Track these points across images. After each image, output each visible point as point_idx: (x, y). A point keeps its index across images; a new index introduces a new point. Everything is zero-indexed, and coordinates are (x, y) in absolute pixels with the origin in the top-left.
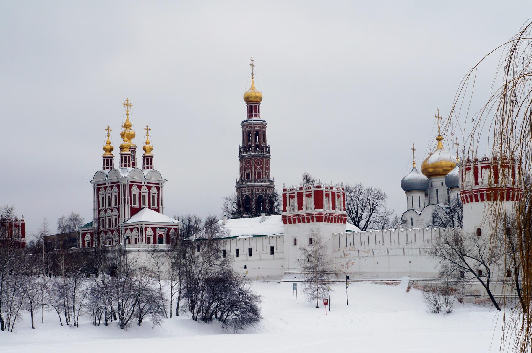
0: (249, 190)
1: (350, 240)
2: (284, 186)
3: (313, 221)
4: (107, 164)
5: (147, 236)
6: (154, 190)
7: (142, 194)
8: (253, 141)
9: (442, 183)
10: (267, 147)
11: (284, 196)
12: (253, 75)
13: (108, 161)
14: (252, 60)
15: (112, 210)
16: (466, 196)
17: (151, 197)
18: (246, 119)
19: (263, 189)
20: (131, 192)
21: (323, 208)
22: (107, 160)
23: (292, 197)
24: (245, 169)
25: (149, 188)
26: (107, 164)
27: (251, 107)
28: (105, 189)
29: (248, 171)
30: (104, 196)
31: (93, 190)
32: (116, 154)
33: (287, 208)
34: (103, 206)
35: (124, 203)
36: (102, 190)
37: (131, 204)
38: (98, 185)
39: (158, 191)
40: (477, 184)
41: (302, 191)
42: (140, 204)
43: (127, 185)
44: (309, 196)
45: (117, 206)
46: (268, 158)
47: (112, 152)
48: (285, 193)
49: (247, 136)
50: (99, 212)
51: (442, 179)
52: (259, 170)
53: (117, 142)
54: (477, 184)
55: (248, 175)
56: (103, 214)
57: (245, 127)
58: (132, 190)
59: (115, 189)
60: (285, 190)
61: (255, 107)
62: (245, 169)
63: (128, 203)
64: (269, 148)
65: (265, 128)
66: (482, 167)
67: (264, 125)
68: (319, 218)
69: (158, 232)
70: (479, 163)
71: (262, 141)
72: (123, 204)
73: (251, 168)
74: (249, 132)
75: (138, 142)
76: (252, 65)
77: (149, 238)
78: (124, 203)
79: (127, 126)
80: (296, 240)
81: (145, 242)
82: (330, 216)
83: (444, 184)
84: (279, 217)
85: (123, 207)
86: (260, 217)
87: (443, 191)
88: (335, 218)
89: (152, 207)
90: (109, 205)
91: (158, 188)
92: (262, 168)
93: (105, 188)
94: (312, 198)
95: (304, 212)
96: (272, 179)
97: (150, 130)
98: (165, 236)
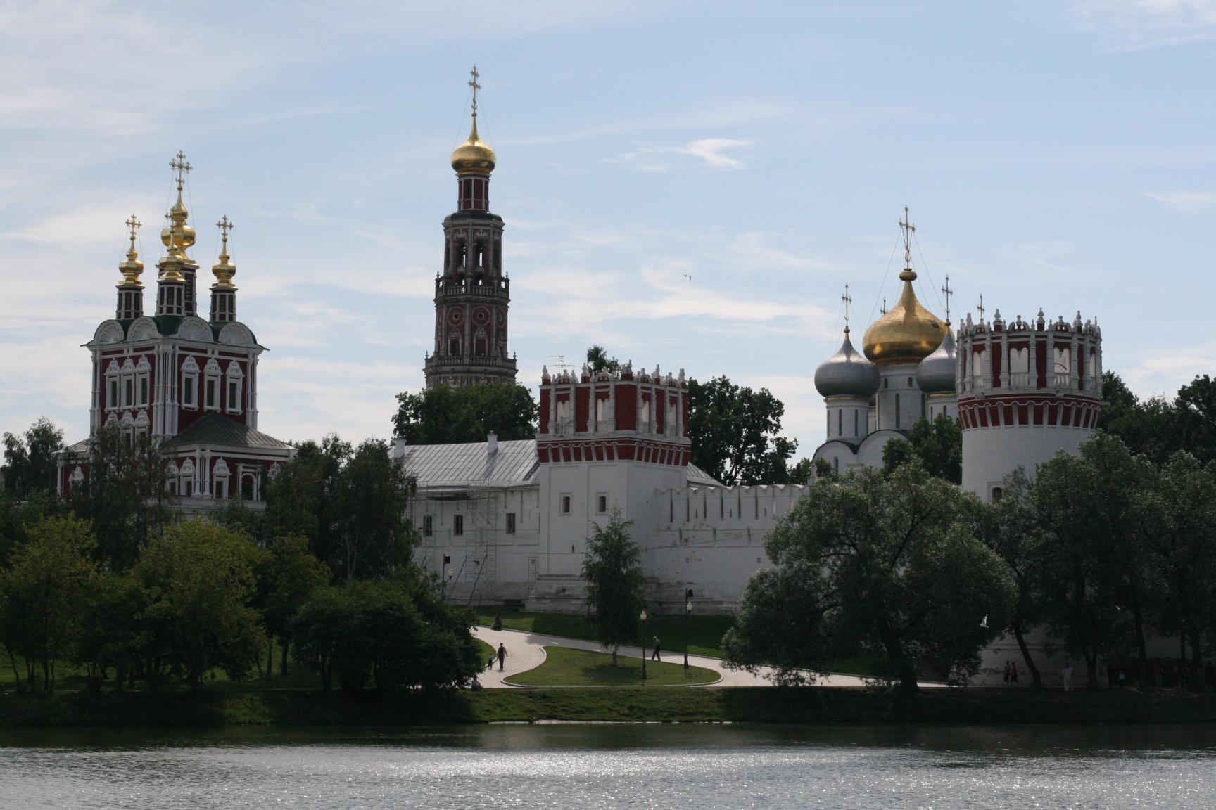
0: (456, 379)
1: (696, 505)
2: (545, 371)
3: (611, 457)
4: (128, 306)
5: (215, 479)
6: (234, 369)
7: (206, 379)
8: (470, 264)
9: (910, 379)
10: (503, 279)
11: (545, 394)
12: (474, 108)
13: (130, 296)
14: (475, 74)
15: (135, 414)
16: (972, 412)
17: (228, 386)
18: (453, 208)
19: (489, 380)
20: (180, 373)
21: (634, 428)
23: (562, 398)
24: (449, 330)
25: (224, 365)
28: (121, 364)
29: (454, 335)
31: (90, 365)
32: (150, 283)
33: (551, 426)
34: (114, 404)
35: (164, 399)
36: (113, 368)
37: (179, 401)
38: (104, 353)
40: (996, 383)
41: (586, 385)
42: (201, 403)
43: (173, 356)
44: (603, 396)
45: (146, 405)
47: (140, 278)
48: (546, 387)
49: (454, 251)
50: (104, 417)
51: (912, 372)
52: (481, 333)
53: (153, 254)
54: (996, 383)
55: (455, 343)
57: (452, 230)
58: (184, 367)
59: (144, 365)
60: (546, 381)
61: (478, 183)
63: (172, 400)
64: (507, 281)
65: (500, 234)
66: (1011, 346)
67: (496, 225)
68: (626, 452)
69: (241, 468)
70: (1004, 337)
71: (491, 264)
72: (161, 402)
73: (462, 330)
74: (462, 243)
75: (203, 257)
76: (474, 85)
77: (220, 484)
78: (164, 399)
79: (179, 216)
80: (567, 500)
81: (211, 491)
82: (652, 448)
83: (915, 382)
84: (531, 445)
86: (487, 444)
87: (910, 402)
88: (663, 452)
89: (228, 409)
91: (244, 366)
92: (488, 330)
93: (121, 362)
94: (611, 402)
95: (590, 434)
96: (510, 357)
97: (231, 226)
98: (257, 483)
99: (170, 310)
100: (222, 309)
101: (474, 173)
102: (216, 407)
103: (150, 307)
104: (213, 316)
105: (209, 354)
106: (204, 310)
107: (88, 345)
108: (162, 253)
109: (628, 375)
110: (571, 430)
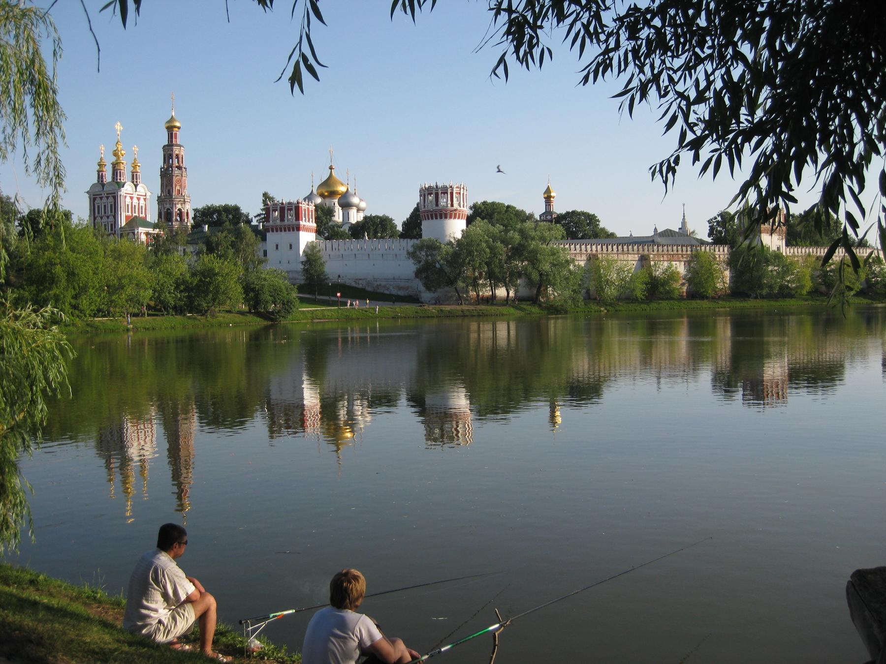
15: (108, 217)
25: (139, 199)
27: (172, 134)
36: (98, 201)
50: (95, 219)
53: (109, 160)
54: (437, 205)
56: (98, 220)
59: (111, 199)
80: (277, 246)
93: (101, 198)
102: (137, 214)
108: (114, 159)
109: (298, 203)
110: (278, 221)
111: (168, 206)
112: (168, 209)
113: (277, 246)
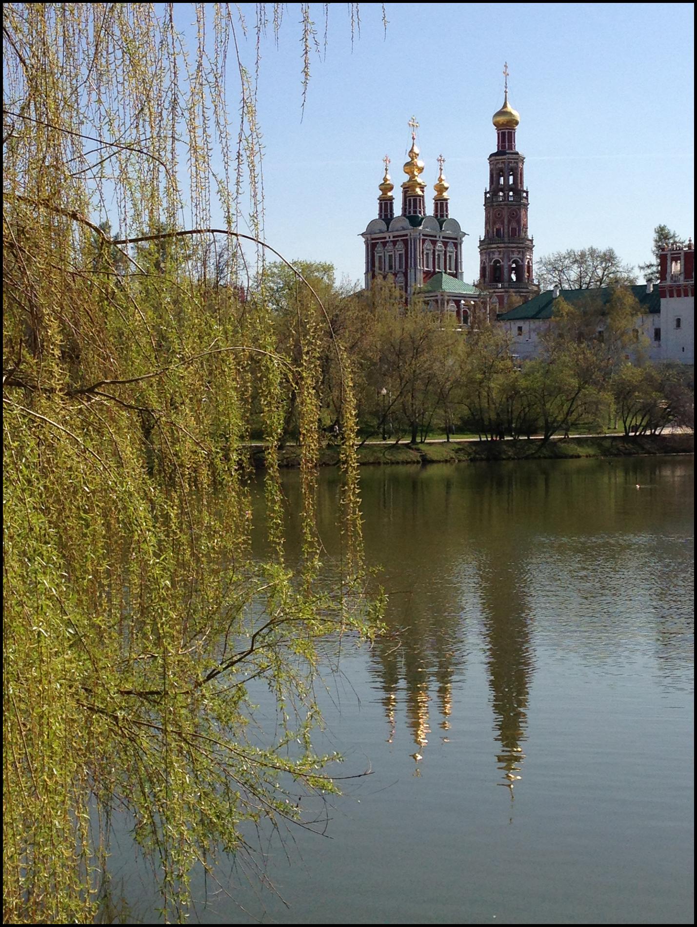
0: (500, 252)
4: (386, 211)
13: (386, 204)
18: (496, 151)
22: (386, 204)
23: (676, 259)
26: (386, 211)
30: (382, 254)
31: (364, 247)
36: (379, 248)
39: (456, 248)
42: (434, 268)
46: (526, 206)
53: (398, 179)
55: (498, 230)
56: (379, 280)
59: (400, 246)
62: (494, 223)
64: (527, 192)
67: (519, 159)
73: (503, 223)
74: (501, 170)
80: (679, 321)
85: (413, 270)
90: (391, 267)
93: (384, 244)
99: (415, 212)
100: (442, 211)
101: (506, 129)
103: (398, 211)
104: (436, 216)
105: (437, 239)
106: (429, 209)
107: (362, 234)
108: (406, 178)
110: (682, 278)
111: (496, 257)
112: (497, 262)
113: (679, 321)
